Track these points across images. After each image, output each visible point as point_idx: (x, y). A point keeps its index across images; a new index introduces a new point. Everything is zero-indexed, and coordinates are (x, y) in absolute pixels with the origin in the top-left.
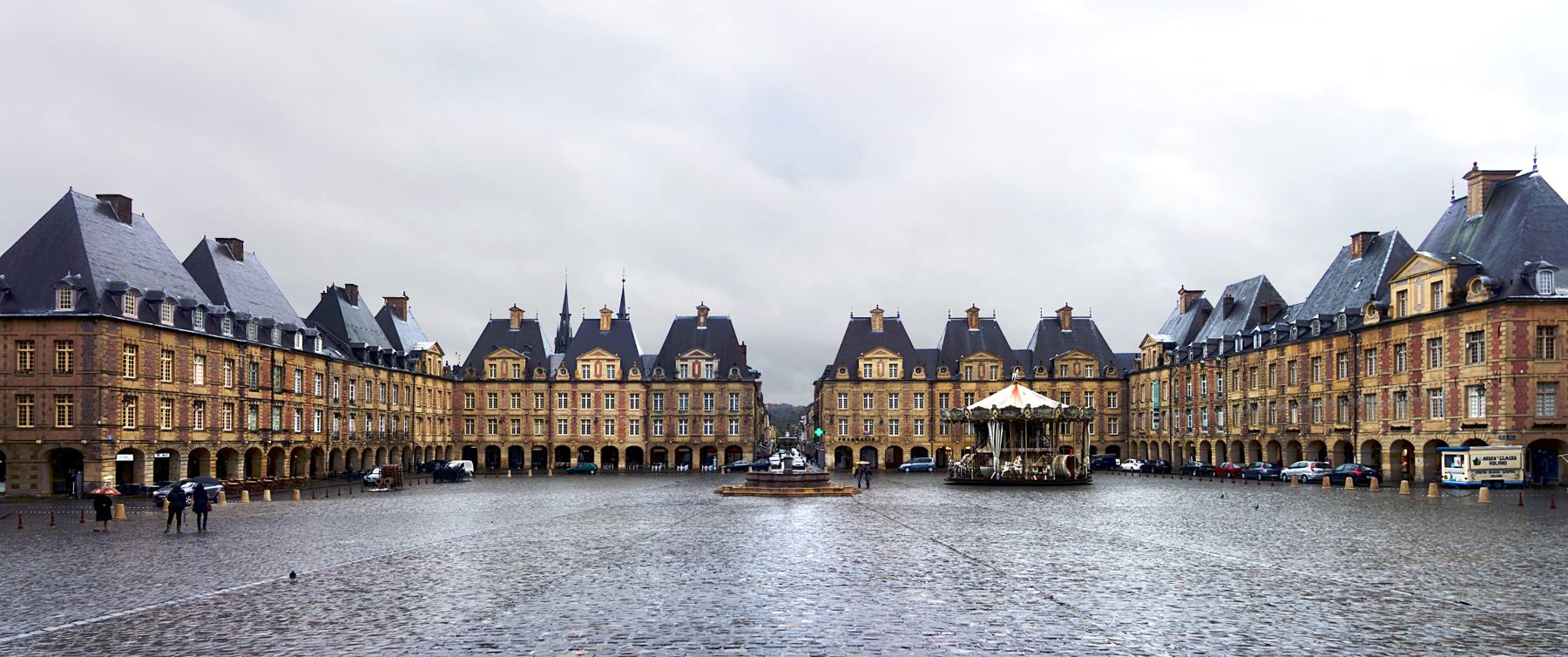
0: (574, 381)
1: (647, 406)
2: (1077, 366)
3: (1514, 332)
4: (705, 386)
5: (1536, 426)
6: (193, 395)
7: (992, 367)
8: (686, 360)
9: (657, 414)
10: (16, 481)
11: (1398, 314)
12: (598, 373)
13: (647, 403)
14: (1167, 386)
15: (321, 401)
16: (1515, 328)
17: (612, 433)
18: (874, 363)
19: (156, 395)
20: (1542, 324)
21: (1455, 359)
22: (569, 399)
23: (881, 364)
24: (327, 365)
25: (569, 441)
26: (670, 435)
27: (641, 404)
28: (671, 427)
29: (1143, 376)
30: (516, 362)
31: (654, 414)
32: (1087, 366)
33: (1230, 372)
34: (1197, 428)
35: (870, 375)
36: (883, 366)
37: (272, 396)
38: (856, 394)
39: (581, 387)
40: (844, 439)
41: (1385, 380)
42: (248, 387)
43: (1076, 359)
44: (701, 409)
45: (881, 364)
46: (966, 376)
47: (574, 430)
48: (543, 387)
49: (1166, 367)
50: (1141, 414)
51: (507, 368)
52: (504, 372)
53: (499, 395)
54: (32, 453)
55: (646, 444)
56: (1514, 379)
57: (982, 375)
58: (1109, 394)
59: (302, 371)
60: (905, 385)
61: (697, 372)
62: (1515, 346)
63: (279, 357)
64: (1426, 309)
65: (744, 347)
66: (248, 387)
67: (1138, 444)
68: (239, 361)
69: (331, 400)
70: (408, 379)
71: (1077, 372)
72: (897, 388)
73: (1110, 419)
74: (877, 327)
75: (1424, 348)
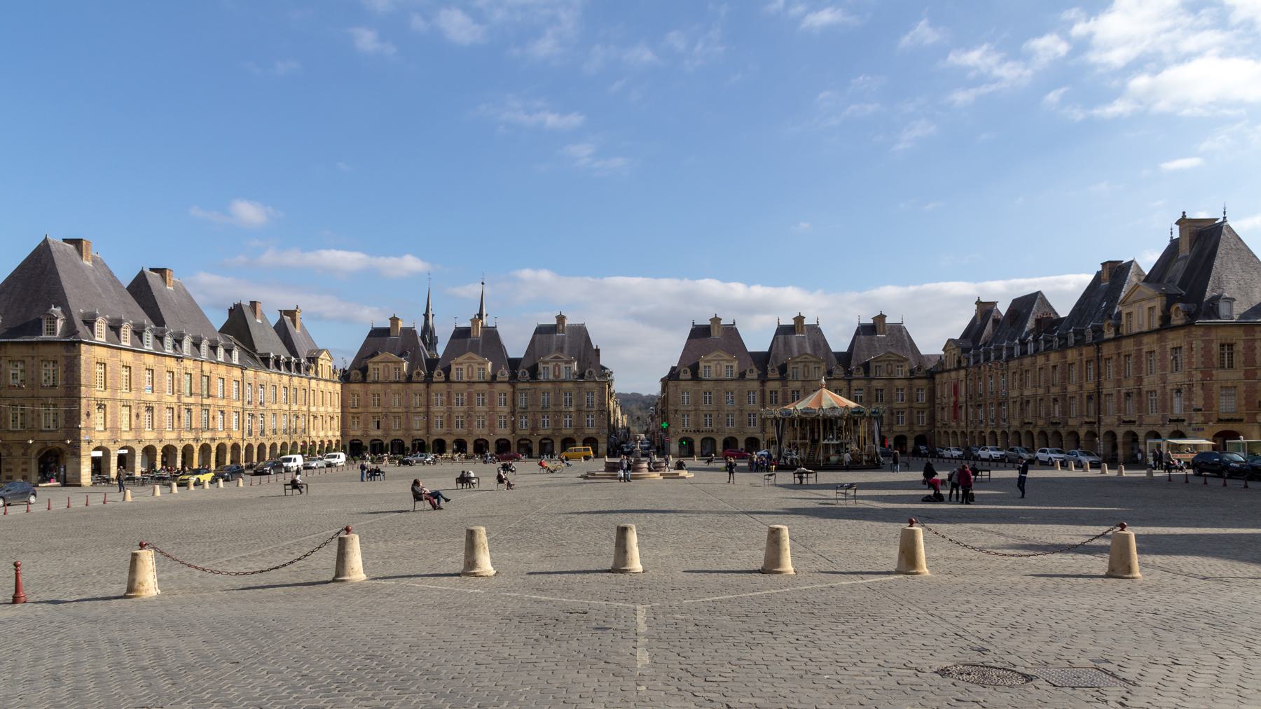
0: (447, 380)
1: (513, 403)
2: (889, 366)
3: (1202, 348)
4: (565, 386)
5: (1220, 421)
6: (145, 402)
7: (815, 368)
8: (547, 363)
9: (522, 410)
10: (9, 474)
11: (1127, 331)
12: (470, 375)
13: (513, 400)
14: (964, 384)
16: (1203, 345)
17: (483, 427)
18: (713, 364)
19: (119, 403)
20: (1224, 342)
21: (1164, 368)
22: (445, 398)
23: (718, 366)
25: (444, 434)
26: (534, 428)
27: (509, 402)
28: (535, 422)
29: (946, 375)
30: (397, 366)
31: (520, 410)
32: (898, 366)
33: (1010, 374)
34: (987, 420)
37: (202, 401)
39: (455, 386)
40: (687, 431)
41: (1119, 383)
43: (890, 360)
44: (561, 405)
45: (718, 366)
46: (793, 376)
47: (449, 425)
48: (422, 386)
49: (963, 368)
50: (943, 408)
51: (388, 370)
52: (387, 375)
53: (382, 396)
54: (23, 451)
55: (514, 437)
56: (1203, 384)
57: (806, 375)
58: (918, 390)
59: (223, 379)
61: (557, 374)
62: (1203, 360)
63: (206, 367)
64: (1145, 329)
65: (597, 351)
67: (942, 433)
68: (178, 373)
69: (246, 403)
70: (305, 381)
71: (890, 371)
72: (733, 386)
73: (918, 412)
75: (1144, 359)
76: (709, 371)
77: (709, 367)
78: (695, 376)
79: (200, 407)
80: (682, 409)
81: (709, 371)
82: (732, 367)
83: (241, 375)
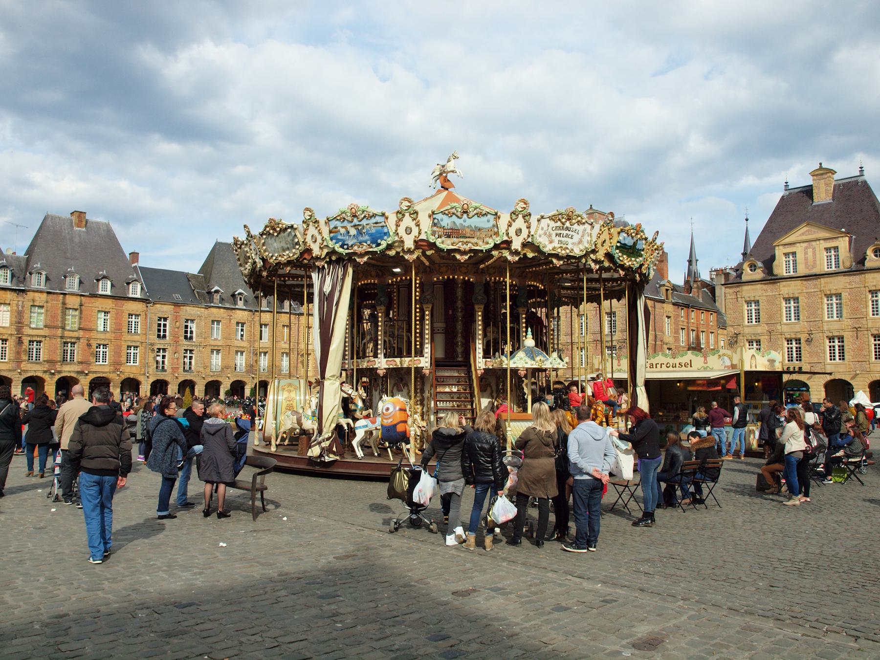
15: (136, 338)
18: (799, 249)
23: (810, 251)
24: (147, 307)
35: (795, 270)
36: (814, 253)
37: (63, 333)
38: (771, 301)
42: (27, 325)
45: (810, 251)
60: (851, 278)
63: (72, 301)
66: (27, 325)
68: (17, 305)
74: (823, 196)
76: (795, 262)
77: (794, 254)
78: (771, 277)
79: (59, 340)
80: (747, 330)
81: (795, 262)
82: (836, 248)
83: (145, 309)
